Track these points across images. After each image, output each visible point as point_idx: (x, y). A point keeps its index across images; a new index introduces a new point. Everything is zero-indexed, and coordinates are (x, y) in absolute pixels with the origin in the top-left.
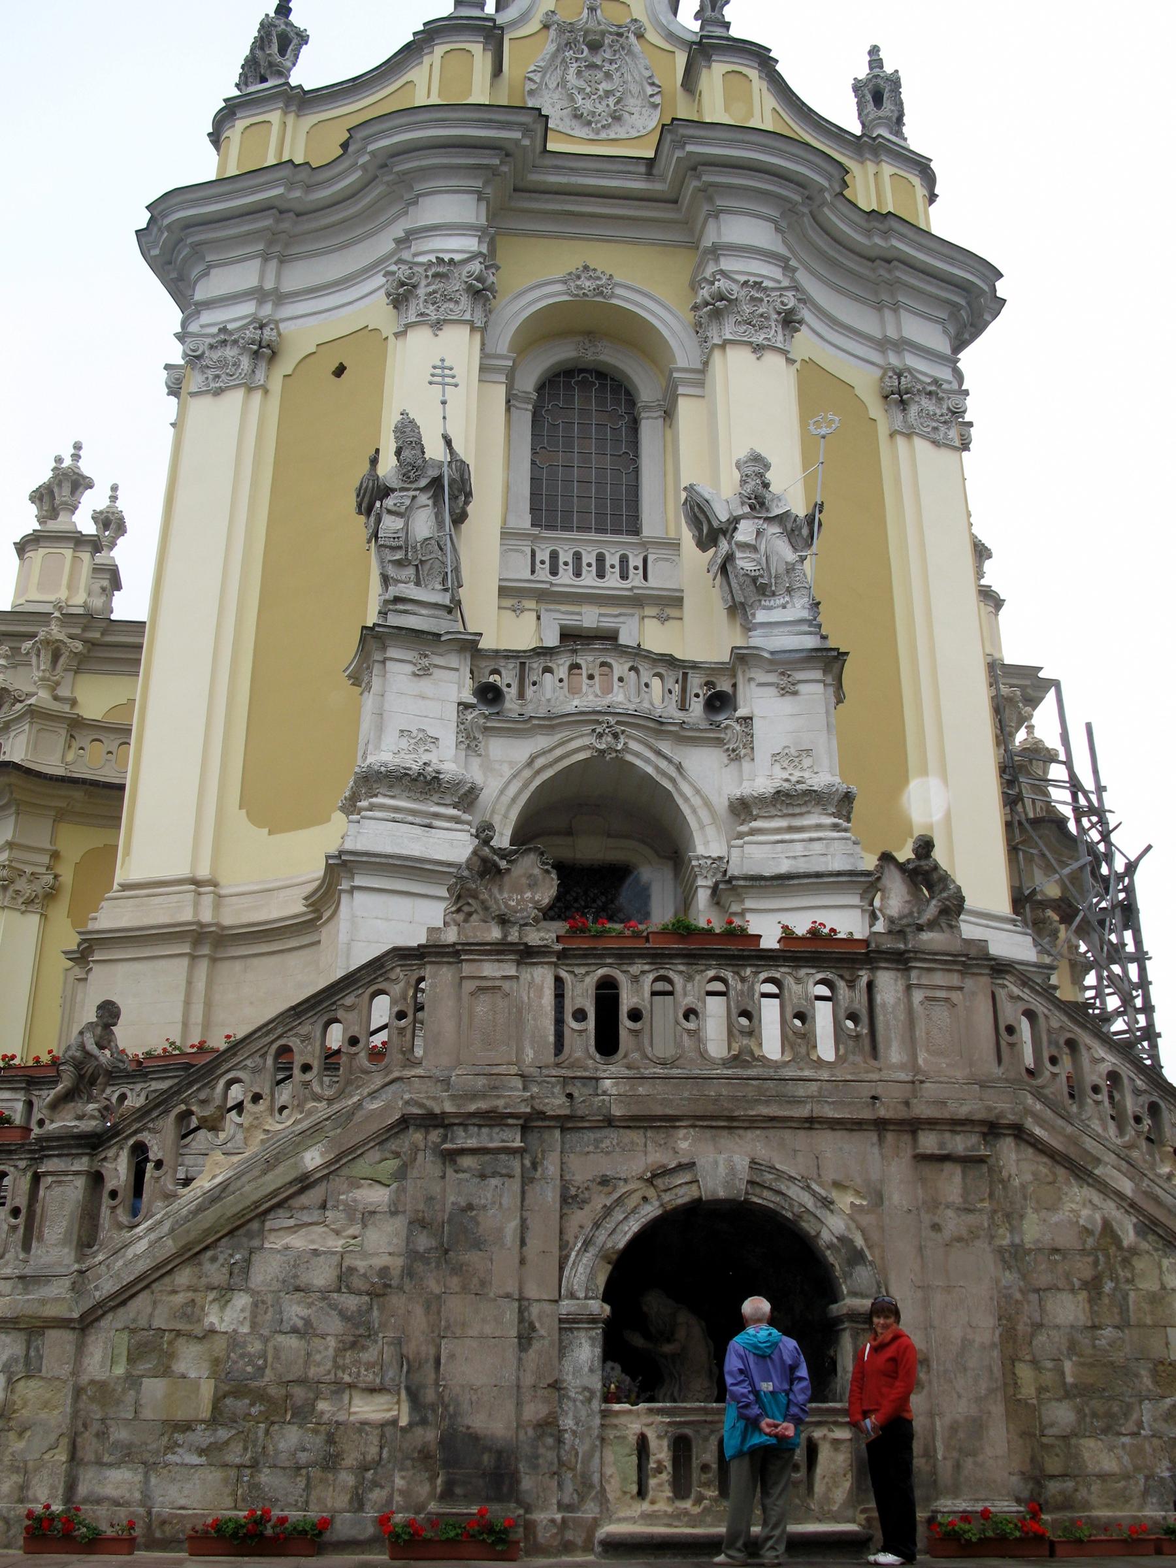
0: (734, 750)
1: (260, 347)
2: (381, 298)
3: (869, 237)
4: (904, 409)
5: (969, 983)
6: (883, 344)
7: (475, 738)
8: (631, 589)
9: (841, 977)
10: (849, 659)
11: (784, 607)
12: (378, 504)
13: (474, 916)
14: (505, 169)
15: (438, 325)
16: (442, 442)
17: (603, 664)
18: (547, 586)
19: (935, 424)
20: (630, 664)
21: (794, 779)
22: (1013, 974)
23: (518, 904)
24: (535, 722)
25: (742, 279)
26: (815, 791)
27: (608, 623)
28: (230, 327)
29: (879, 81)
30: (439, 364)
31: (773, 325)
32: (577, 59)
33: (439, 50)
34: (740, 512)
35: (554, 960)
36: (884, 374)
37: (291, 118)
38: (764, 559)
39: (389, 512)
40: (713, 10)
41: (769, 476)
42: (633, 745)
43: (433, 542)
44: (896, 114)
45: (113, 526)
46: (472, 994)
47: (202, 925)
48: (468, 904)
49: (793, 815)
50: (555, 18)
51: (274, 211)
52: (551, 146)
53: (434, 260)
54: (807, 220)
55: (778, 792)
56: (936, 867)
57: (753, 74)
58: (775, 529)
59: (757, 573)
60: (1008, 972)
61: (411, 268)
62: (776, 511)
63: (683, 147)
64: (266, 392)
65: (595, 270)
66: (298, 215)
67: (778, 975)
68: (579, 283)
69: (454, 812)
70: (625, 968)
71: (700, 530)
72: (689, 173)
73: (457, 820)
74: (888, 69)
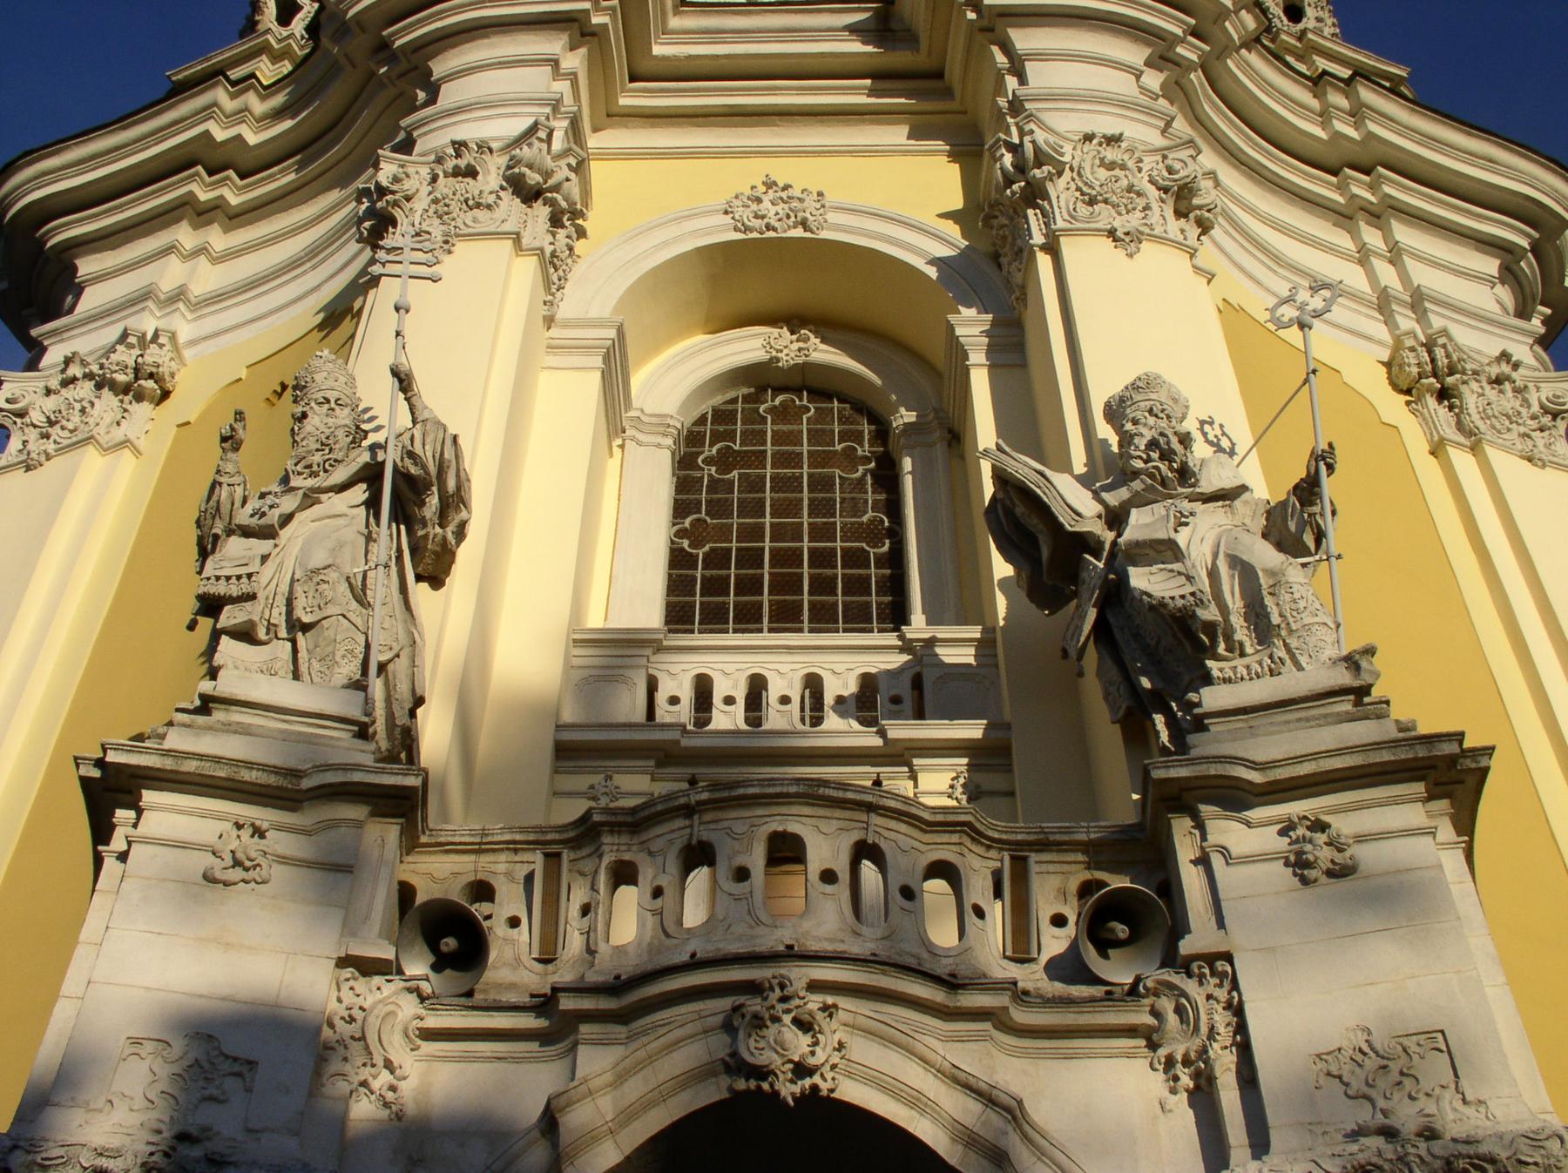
1: (137, 378)
7: (389, 1065)
10: (1496, 763)
16: (389, 382)
19: (1522, 429)
20: (856, 836)
31: (1155, 206)
42: (865, 1052)
43: (332, 575)
54: (1196, 77)
65: (786, 187)
71: (1038, 561)
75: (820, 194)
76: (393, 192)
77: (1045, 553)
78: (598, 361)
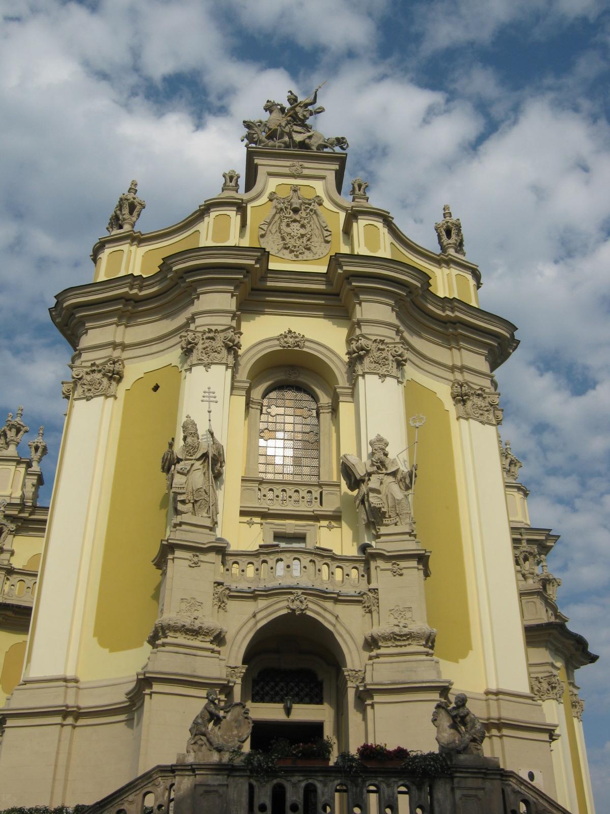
0: (368, 607)
2: (178, 352)
3: (444, 312)
4: (464, 404)
5: (488, 784)
6: (453, 369)
7: (223, 602)
8: (313, 512)
9: (413, 783)
11: (396, 524)
12: (173, 466)
13: (204, 747)
14: (247, 280)
15: (207, 366)
17: (295, 559)
18: (267, 510)
19: (481, 412)
20: (311, 558)
21: (401, 625)
22: (515, 778)
23: (229, 738)
24: (257, 593)
25: (374, 338)
26: (413, 632)
27: (300, 530)
28: (98, 362)
29: (449, 224)
30: (207, 390)
31: (390, 362)
32: (287, 218)
33: (213, 214)
34: (372, 470)
35: (249, 774)
36: (453, 385)
37: (134, 248)
38: (385, 497)
39: (178, 472)
40: (359, 190)
41: (387, 449)
42: (311, 605)
43: (202, 490)
44: (459, 241)
45: (40, 450)
46: (201, 795)
47: (67, 707)
48: (201, 739)
49: (401, 646)
50: (275, 196)
51: (123, 300)
52: (272, 266)
53: (207, 330)
55: (392, 633)
56: (468, 713)
57: (380, 225)
58: (391, 479)
59: (381, 506)
60: (511, 776)
61: (194, 334)
62: (391, 469)
63: (341, 268)
64: (116, 398)
65: (295, 333)
66: (136, 302)
67: (376, 783)
68: (285, 340)
69: (211, 646)
70: (289, 778)
72: (345, 281)
73: (213, 651)
74: (454, 218)
75: (303, 336)
76: (192, 343)
77: (353, 480)
78: (244, 393)
